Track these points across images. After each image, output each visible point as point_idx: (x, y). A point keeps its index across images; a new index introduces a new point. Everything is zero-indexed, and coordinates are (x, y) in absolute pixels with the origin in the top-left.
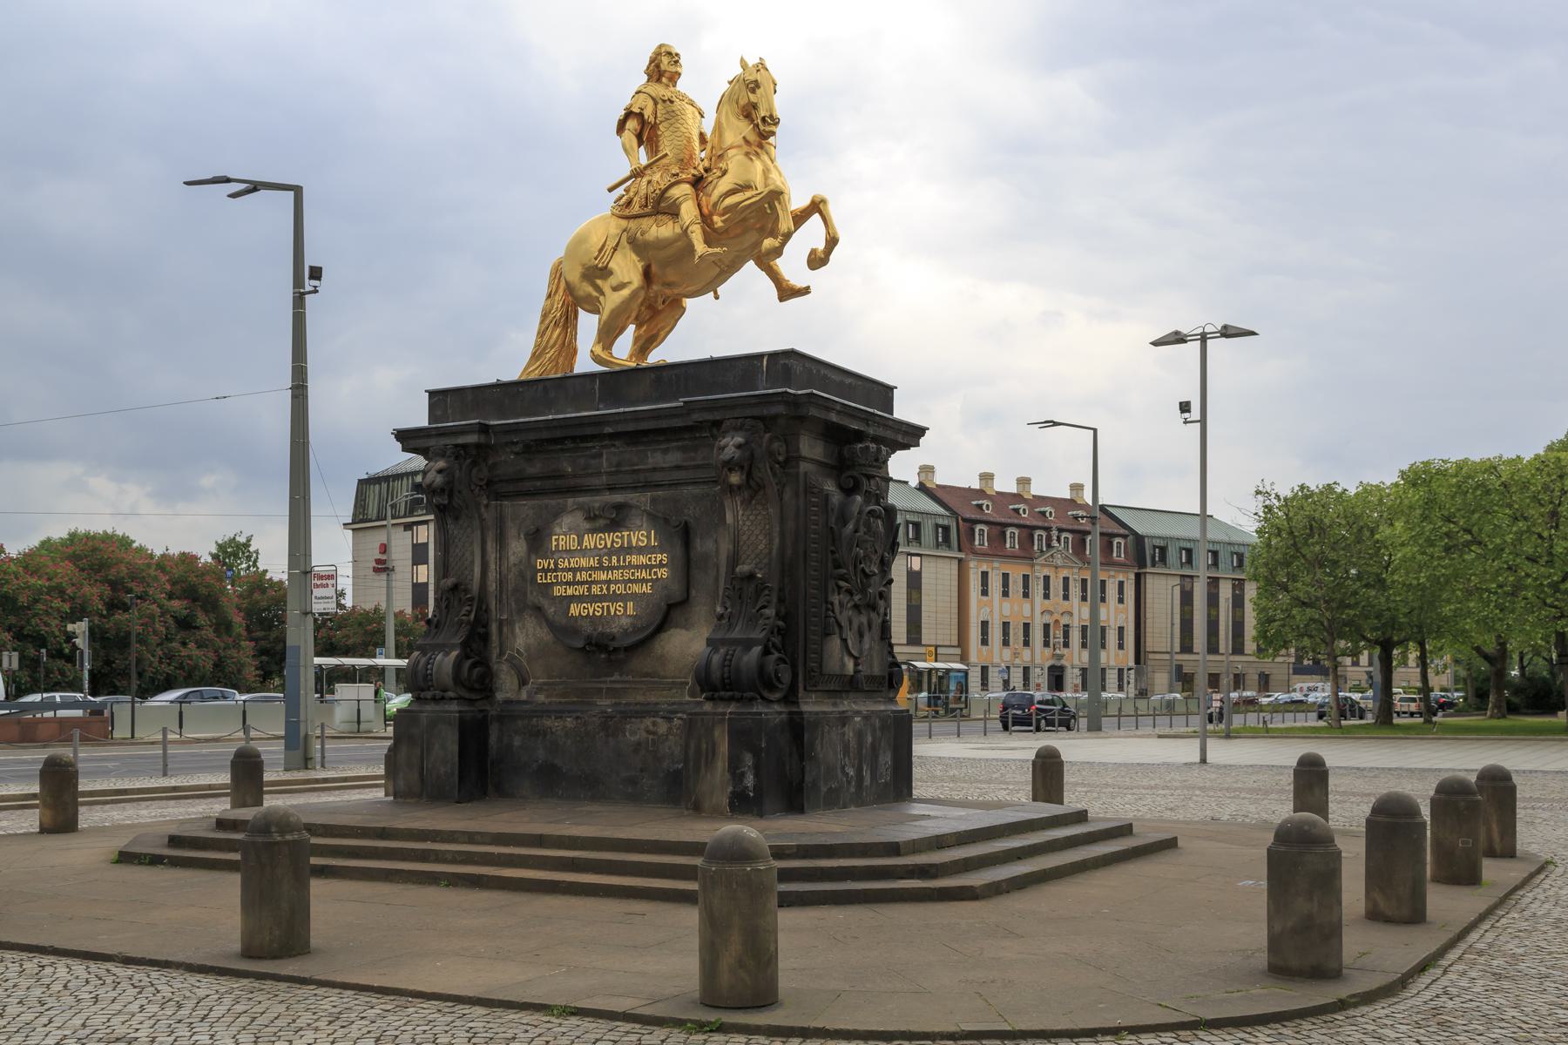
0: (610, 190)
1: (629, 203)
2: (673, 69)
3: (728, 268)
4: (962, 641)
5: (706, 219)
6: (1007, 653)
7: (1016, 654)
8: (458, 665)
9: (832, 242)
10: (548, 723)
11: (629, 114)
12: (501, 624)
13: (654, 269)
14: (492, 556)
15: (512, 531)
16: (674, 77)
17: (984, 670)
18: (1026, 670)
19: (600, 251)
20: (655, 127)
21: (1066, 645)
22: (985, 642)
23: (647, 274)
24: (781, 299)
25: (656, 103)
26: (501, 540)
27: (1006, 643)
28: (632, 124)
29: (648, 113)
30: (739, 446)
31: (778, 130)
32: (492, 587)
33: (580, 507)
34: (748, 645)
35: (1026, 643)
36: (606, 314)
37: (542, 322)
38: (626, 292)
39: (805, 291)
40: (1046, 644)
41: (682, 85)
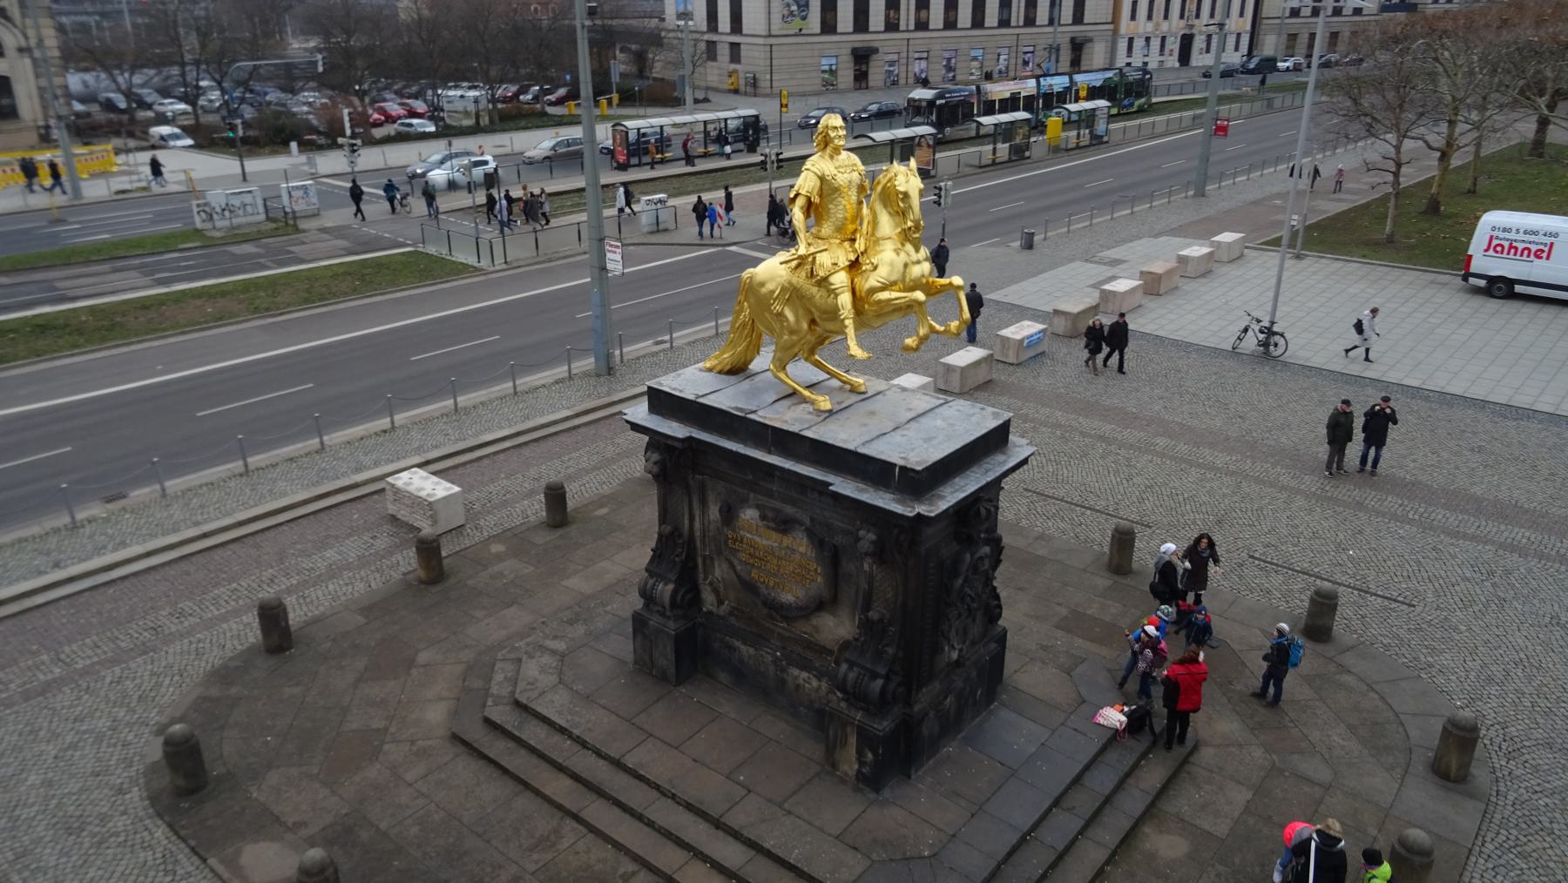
4: (1115, 20)
6: (1150, 26)
7: (1157, 25)
8: (675, 592)
10: (738, 644)
12: (704, 558)
14: (697, 513)
15: (711, 497)
17: (1131, 40)
18: (1163, 39)
21: (1198, 16)
22: (1133, 17)
26: (704, 503)
27: (1150, 17)
30: (873, 542)
32: (698, 534)
33: (758, 507)
34: (874, 676)
35: (1166, 17)
40: (1182, 17)
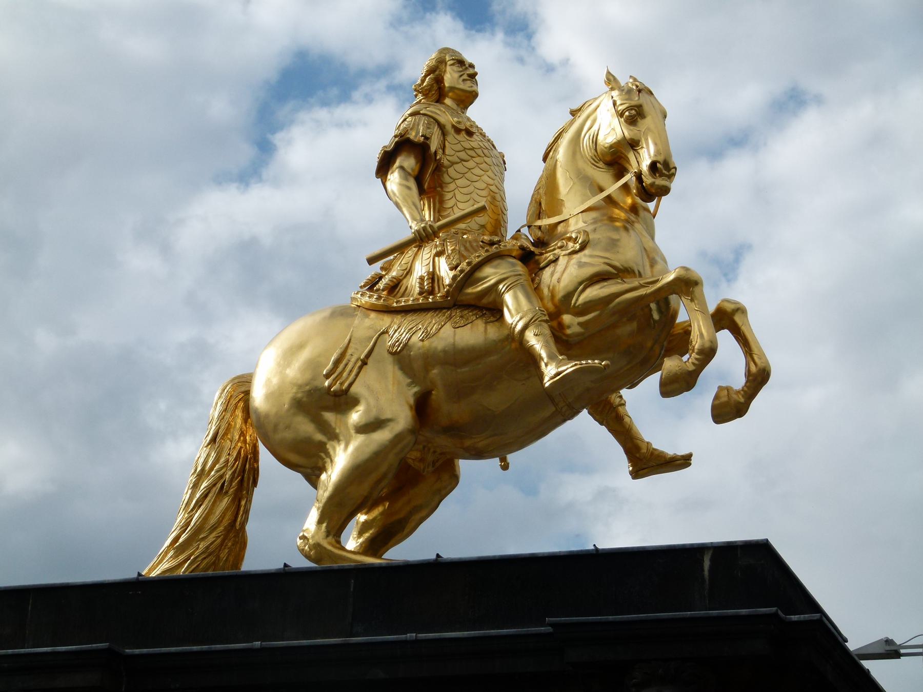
0: (372, 261)
1: (394, 287)
2: (467, 86)
3: (558, 406)
5: (551, 318)
9: (758, 378)
11: (402, 144)
13: (438, 395)
16: (467, 98)
19: (337, 363)
20: (439, 168)
23: (422, 407)
24: (637, 474)
25: (444, 133)
28: (407, 161)
29: (434, 146)
31: (676, 185)
36: (332, 475)
37: (196, 486)
38: (382, 436)
39: (683, 462)
41: (474, 113)
